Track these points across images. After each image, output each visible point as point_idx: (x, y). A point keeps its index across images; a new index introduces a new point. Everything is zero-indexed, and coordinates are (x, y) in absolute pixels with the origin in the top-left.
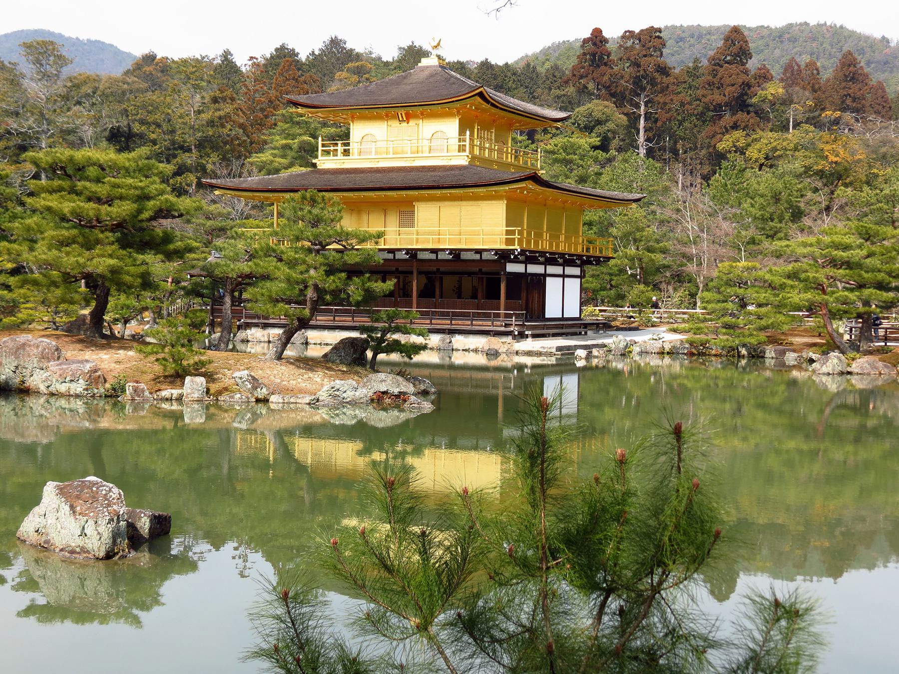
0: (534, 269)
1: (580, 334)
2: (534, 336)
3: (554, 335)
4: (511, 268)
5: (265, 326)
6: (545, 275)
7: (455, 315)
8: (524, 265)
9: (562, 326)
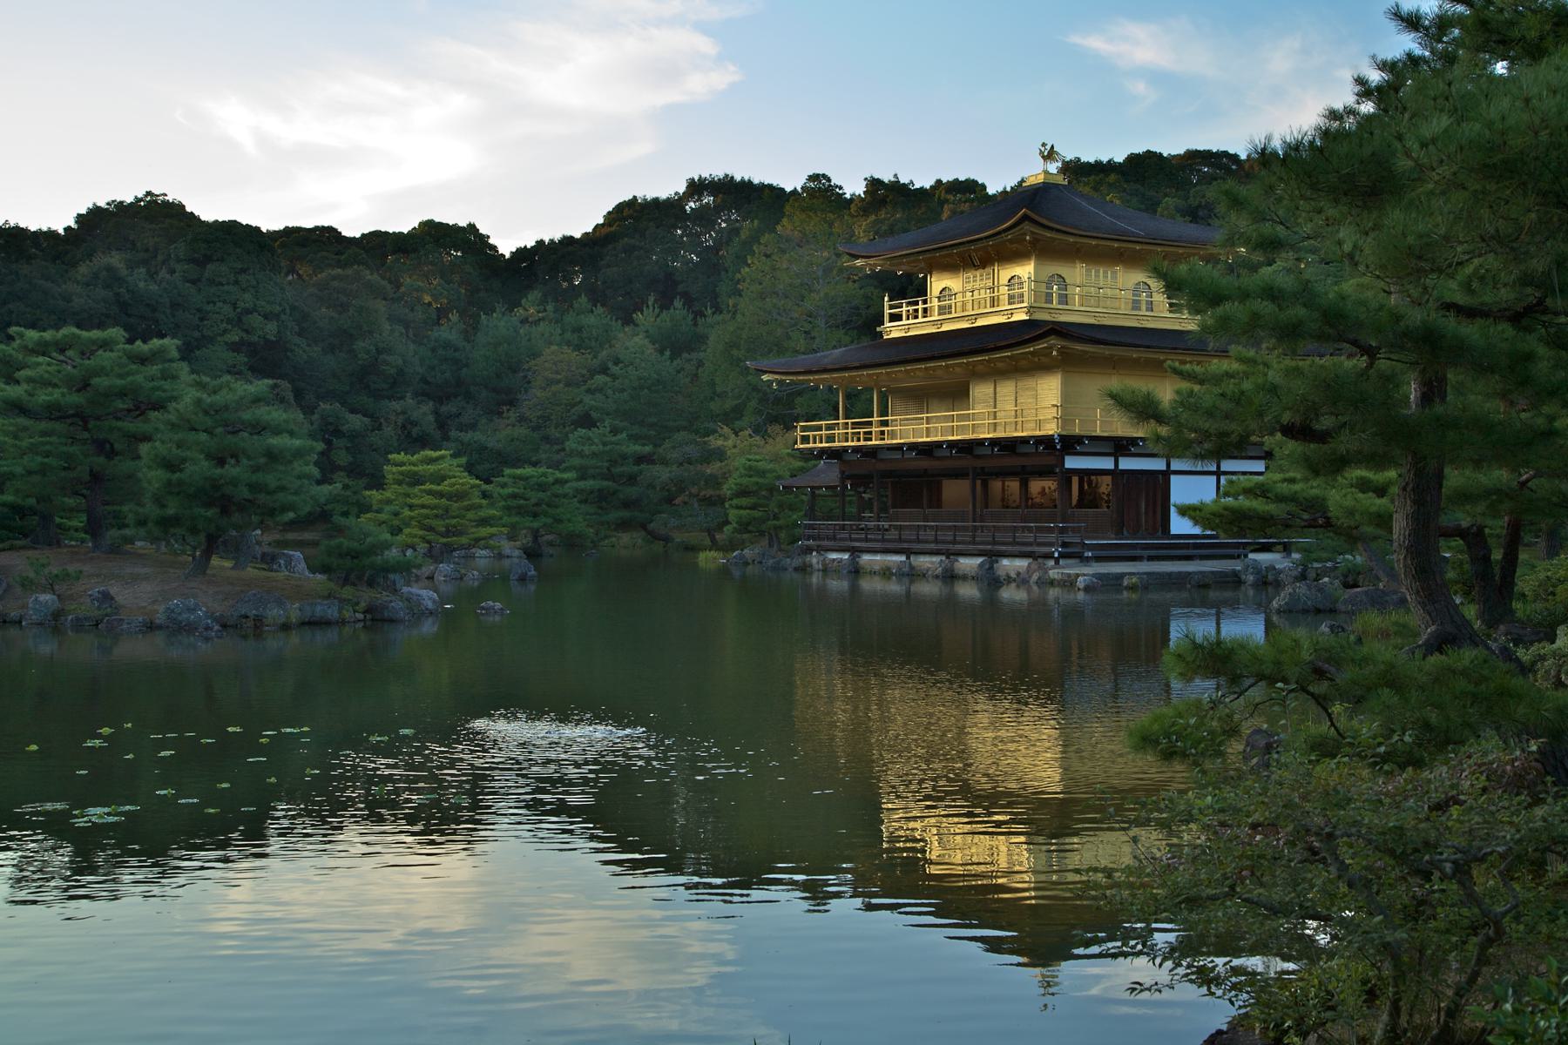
0: (1127, 464)
1: (1239, 557)
2: (1098, 559)
3: (1151, 558)
4: (1072, 463)
5: (820, 550)
6: (1167, 474)
7: (1039, 530)
8: (1112, 459)
9: (1187, 546)
